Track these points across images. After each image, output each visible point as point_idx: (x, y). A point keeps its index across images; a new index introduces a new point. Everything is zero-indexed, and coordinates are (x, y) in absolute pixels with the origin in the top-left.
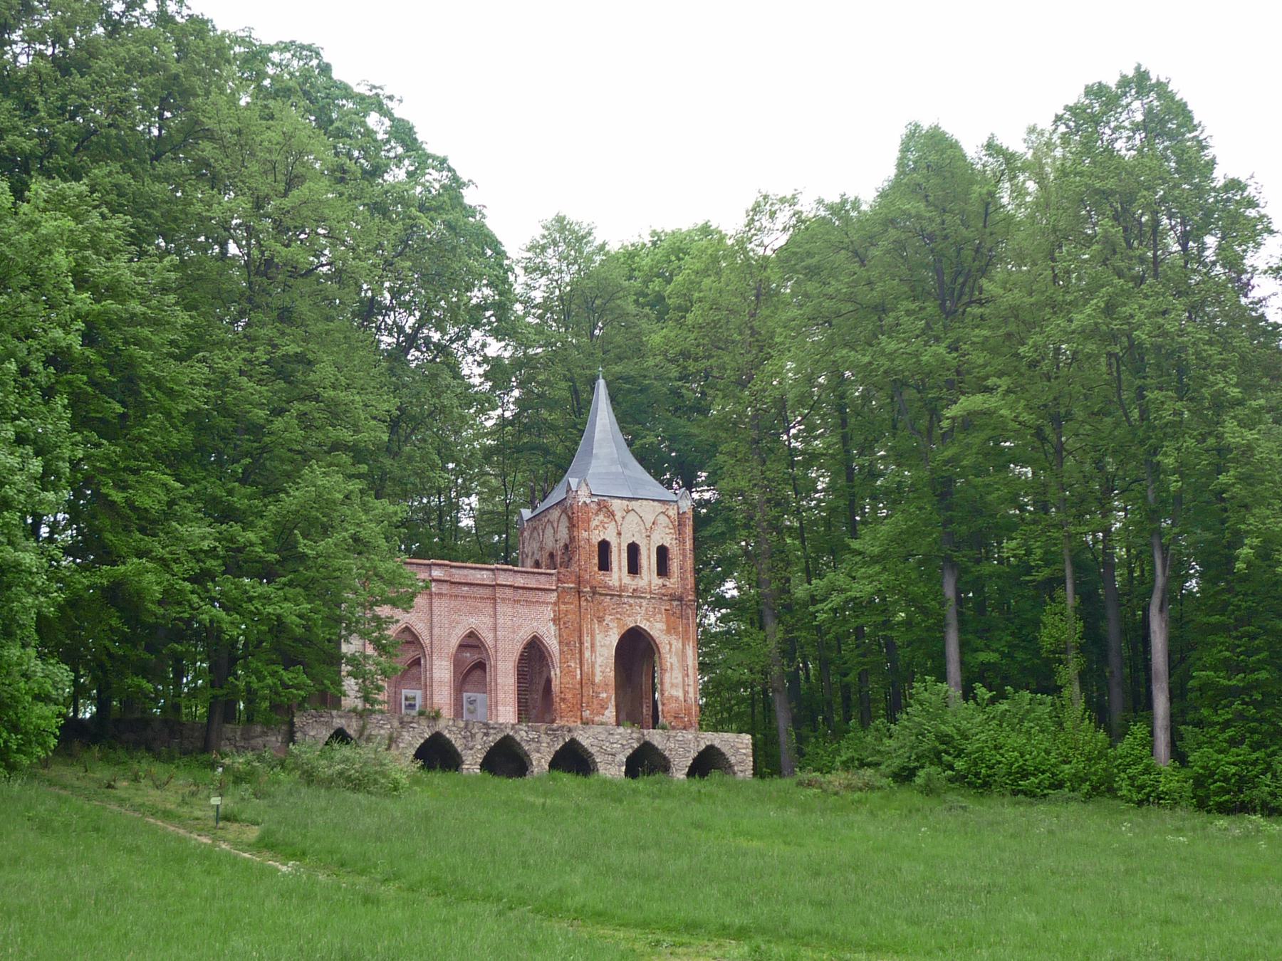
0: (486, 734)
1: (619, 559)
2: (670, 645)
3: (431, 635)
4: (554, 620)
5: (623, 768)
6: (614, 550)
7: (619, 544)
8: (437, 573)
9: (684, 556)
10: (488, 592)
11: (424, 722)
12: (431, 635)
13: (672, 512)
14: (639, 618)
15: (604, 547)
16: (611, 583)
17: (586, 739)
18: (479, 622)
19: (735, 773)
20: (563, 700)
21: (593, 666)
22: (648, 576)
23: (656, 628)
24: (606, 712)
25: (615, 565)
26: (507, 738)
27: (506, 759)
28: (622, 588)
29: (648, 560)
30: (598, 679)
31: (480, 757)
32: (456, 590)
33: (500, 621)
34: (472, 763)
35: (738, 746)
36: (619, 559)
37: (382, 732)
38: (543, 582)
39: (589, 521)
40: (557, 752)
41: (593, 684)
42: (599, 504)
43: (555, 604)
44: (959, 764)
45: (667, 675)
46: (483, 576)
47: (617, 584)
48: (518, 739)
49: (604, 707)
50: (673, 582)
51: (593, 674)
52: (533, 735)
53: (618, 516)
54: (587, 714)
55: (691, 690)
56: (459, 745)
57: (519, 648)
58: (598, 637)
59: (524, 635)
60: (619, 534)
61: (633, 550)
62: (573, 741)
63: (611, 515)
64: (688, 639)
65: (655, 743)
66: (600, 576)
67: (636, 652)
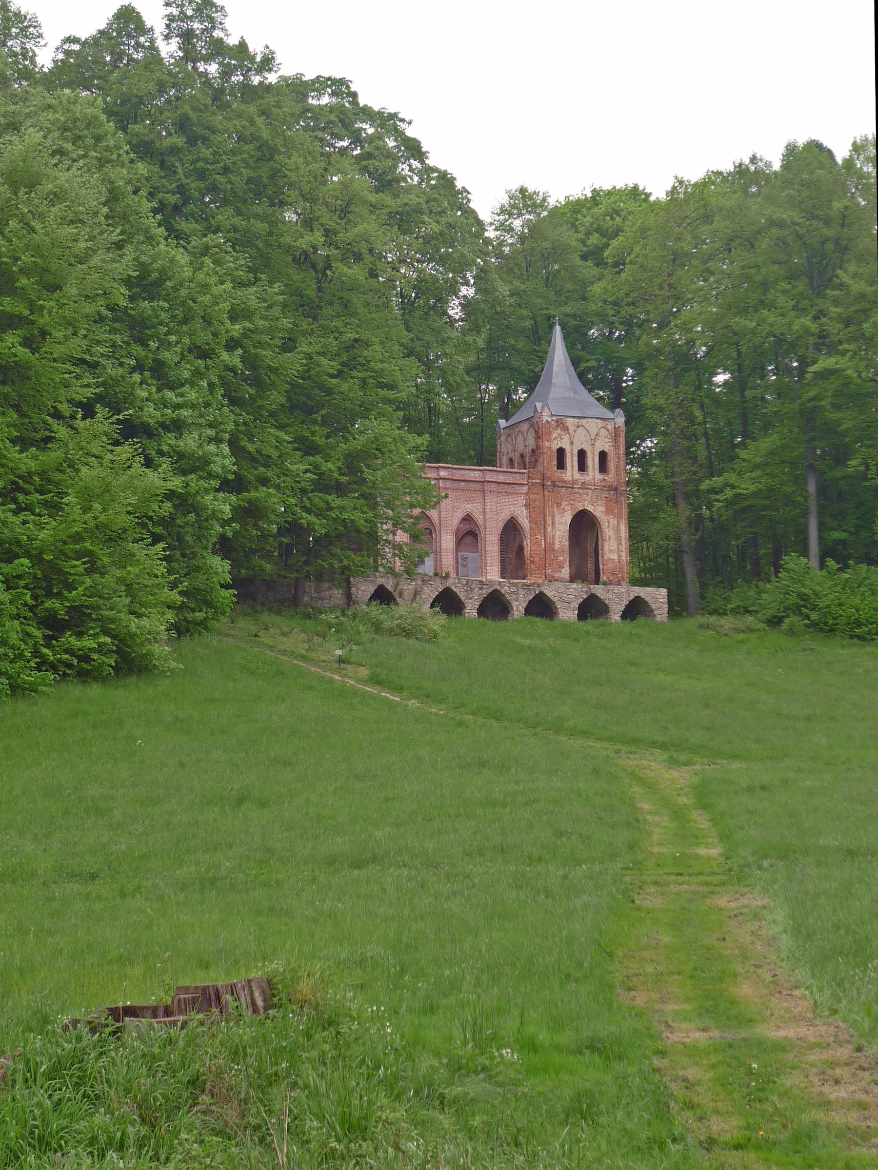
0: (481, 589)
1: (571, 461)
2: (609, 522)
3: (440, 518)
4: (525, 506)
5: (576, 612)
6: (568, 455)
7: (572, 450)
8: (443, 473)
9: (619, 458)
10: (479, 486)
11: (438, 580)
12: (440, 518)
13: (610, 427)
14: (586, 503)
15: (561, 452)
17: (549, 592)
18: (473, 508)
19: (654, 616)
20: (532, 562)
21: (554, 538)
22: (593, 473)
23: (598, 511)
25: (569, 465)
26: (496, 591)
27: (495, 606)
28: (574, 482)
29: (593, 461)
30: (557, 546)
31: (477, 604)
32: (456, 485)
33: (488, 507)
34: (471, 609)
35: (657, 597)
36: (571, 461)
37: (410, 587)
38: (517, 479)
39: (550, 433)
40: (530, 601)
41: (553, 550)
42: (557, 421)
43: (526, 494)
44: (814, 616)
45: (607, 544)
46: (476, 475)
47: (570, 479)
48: (503, 592)
49: (561, 567)
50: (611, 477)
51: (554, 544)
52: (513, 589)
53: (571, 429)
54: (549, 571)
55: (623, 554)
56: (462, 596)
57: (501, 525)
58: (557, 517)
59: (505, 516)
60: (572, 443)
61: (582, 454)
62: (541, 593)
63: (566, 429)
64: (622, 518)
65: (599, 595)
66: (559, 473)
67: (584, 526)
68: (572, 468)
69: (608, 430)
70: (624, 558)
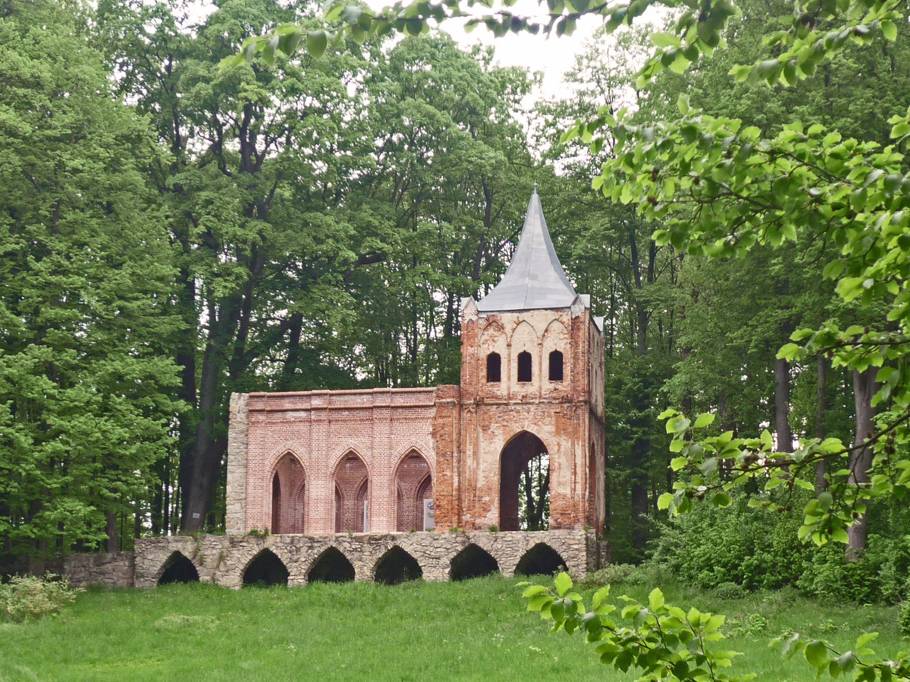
1: (509, 369)
2: (559, 445)
8: (316, 402)
14: (526, 423)
16: (499, 393)
18: (358, 443)
23: (544, 432)
24: (489, 515)
29: (540, 367)
30: (479, 485)
32: (335, 415)
36: (509, 369)
38: (423, 400)
42: (487, 320)
47: (505, 393)
50: (565, 386)
51: (476, 481)
53: (508, 328)
59: (402, 449)
60: (509, 345)
61: (525, 360)
63: (501, 328)
68: (509, 379)
69: (563, 323)
70: (579, 491)
